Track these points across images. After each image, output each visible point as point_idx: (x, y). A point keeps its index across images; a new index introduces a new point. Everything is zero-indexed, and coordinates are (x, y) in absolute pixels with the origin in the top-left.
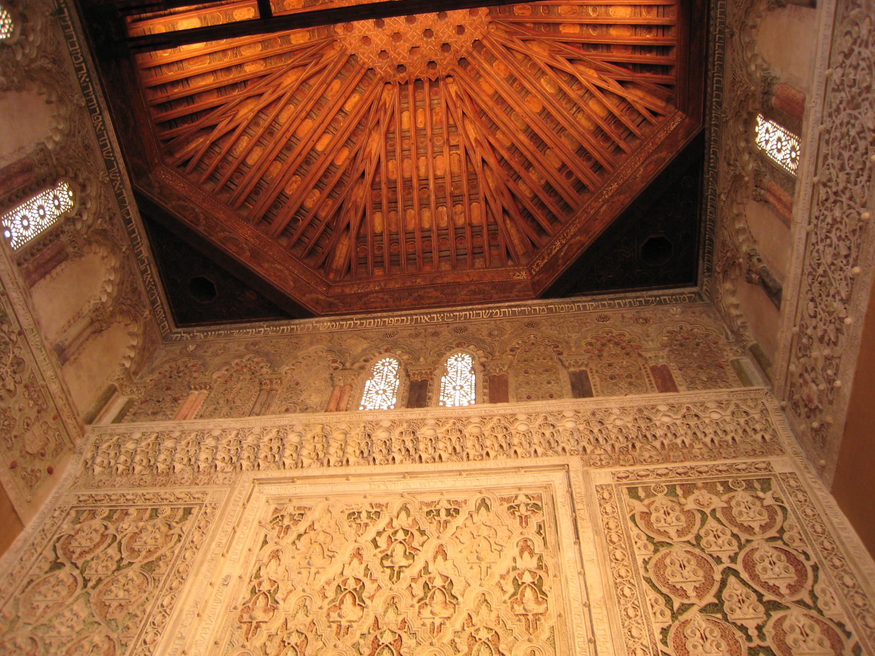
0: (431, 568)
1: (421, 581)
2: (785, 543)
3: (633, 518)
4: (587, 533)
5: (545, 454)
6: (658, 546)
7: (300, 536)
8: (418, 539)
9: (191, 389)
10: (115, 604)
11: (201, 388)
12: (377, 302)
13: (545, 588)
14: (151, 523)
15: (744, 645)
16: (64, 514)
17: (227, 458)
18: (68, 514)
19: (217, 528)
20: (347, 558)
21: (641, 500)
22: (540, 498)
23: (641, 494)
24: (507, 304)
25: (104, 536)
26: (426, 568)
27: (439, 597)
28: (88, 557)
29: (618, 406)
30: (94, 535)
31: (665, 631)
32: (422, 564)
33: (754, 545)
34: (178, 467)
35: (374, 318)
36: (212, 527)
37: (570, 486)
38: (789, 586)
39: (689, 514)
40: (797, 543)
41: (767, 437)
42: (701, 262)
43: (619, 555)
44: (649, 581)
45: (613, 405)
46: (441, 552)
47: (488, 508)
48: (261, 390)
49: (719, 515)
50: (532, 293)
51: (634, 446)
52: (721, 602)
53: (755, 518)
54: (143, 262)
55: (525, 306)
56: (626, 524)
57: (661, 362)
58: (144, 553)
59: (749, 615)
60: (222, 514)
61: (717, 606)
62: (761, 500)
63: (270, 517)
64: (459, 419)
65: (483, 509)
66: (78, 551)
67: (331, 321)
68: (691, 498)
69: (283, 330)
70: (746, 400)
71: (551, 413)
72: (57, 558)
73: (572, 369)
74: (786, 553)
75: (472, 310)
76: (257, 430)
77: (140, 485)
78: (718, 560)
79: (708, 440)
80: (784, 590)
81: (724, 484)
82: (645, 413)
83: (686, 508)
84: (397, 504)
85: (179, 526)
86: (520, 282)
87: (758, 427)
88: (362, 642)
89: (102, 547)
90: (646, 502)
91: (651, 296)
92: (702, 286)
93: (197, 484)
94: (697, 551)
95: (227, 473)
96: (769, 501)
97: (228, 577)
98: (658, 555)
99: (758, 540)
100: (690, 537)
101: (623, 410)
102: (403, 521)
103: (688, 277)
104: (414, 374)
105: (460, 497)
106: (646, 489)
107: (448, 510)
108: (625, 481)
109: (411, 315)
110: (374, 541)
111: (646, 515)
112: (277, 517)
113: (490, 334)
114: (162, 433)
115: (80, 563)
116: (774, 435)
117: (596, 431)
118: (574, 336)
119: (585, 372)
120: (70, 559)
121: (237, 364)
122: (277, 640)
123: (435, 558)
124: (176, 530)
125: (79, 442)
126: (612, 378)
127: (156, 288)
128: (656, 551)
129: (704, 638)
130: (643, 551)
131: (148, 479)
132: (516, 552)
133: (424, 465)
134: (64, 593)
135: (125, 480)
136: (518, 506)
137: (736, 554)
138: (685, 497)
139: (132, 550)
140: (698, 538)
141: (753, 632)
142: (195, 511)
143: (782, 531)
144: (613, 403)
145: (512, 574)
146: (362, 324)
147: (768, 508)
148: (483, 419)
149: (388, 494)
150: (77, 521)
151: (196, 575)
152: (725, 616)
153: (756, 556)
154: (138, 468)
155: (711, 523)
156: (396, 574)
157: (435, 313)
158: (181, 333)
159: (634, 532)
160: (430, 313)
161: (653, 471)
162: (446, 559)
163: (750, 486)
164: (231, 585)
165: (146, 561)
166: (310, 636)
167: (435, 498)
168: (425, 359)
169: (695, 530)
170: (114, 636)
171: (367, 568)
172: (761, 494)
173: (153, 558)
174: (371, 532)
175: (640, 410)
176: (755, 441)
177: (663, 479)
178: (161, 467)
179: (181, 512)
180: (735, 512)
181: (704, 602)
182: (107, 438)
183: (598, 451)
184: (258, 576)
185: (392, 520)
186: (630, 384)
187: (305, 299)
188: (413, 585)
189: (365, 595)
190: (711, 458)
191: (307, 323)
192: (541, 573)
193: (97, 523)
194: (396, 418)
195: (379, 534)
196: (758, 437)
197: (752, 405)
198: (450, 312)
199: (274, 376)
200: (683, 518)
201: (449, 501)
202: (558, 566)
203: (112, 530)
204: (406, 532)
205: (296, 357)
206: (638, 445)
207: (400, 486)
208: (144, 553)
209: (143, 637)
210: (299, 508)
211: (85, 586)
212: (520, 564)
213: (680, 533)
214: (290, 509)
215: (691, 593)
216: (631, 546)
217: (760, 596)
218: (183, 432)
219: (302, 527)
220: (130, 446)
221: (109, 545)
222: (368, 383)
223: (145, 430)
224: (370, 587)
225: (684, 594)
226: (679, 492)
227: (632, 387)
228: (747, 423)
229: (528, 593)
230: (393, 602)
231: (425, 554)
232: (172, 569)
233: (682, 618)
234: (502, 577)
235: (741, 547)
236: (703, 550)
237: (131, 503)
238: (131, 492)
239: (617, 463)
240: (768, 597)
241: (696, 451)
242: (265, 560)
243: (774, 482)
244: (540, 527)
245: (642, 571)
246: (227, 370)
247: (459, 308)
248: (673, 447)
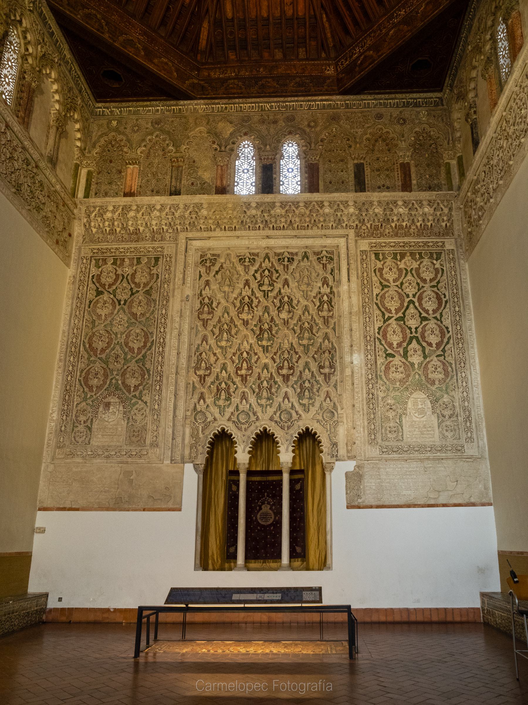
0: (282, 291)
1: (279, 298)
2: (438, 289)
3: (375, 271)
4: (354, 278)
5: (336, 228)
6: (384, 287)
7: (217, 272)
8: (275, 275)
9: (127, 164)
10: (139, 314)
11: (134, 164)
12: (234, 88)
13: (333, 304)
14: (139, 266)
15: (409, 335)
16: (89, 261)
17: (168, 224)
18: (91, 261)
19: (175, 271)
20: (241, 286)
21: (380, 261)
22: (333, 253)
23: (381, 257)
24: (320, 98)
25: (117, 276)
26: (280, 291)
27: (286, 307)
28: (114, 287)
29: (377, 199)
30: (111, 274)
31: (379, 328)
32: (278, 290)
33: (425, 289)
34: (141, 229)
35: (234, 104)
36: (172, 269)
37: (347, 247)
38: (433, 310)
39: (400, 270)
40: (443, 289)
41: (448, 225)
42: (447, 79)
43: (366, 291)
44: (377, 304)
45: (375, 199)
46: (286, 283)
47: (308, 259)
48: (172, 166)
49: (414, 272)
50: (335, 88)
51: (382, 225)
52: (405, 316)
53: (428, 276)
54: (67, 62)
55: (331, 100)
56: (371, 274)
57: (407, 160)
58: (142, 285)
59: (413, 323)
60: (176, 261)
61: (402, 319)
62: (434, 264)
63: (199, 261)
64: (293, 203)
65: (305, 259)
66: (107, 284)
67: (205, 104)
68: (403, 261)
69: (174, 109)
70: (444, 201)
71: (341, 202)
72: (98, 288)
73: (356, 162)
74: (437, 294)
75: (297, 101)
76: (181, 206)
77: (123, 241)
78: (408, 296)
79: (418, 224)
80: (431, 312)
81: (420, 254)
82: (391, 205)
83: (400, 267)
84: (263, 255)
85: (155, 268)
86: (329, 77)
87: (445, 218)
88: (255, 328)
89: (119, 282)
90: (382, 263)
91: (411, 99)
92: (444, 94)
93: (156, 241)
94: (400, 290)
95: (170, 233)
96: (438, 266)
97: (188, 296)
98: (383, 292)
99: (427, 286)
100: (398, 283)
101: (379, 202)
102: (266, 264)
103: (436, 85)
104: (264, 159)
105: (294, 251)
106: (383, 254)
107: (288, 258)
108: (374, 249)
109: (258, 103)
110: (254, 275)
111: (381, 270)
112: (203, 262)
113: (309, 126)
114: (125, 206)
115: (111, 290)
116: (452, 223)
117: (364, 214)
118: (360, 131)
119: (363, 164)
120: (105, 288)
121: (150, 139)
122: (218, 327)
123: (284, 286)
124: (154, 271)
125: (75, 211)
126: (378, 170)
127: (80, 79)
128: (382, 289)
129: (394, 332)
130: (377, 290)
131: (126, 236)
132: (320, 284)
133: (275, 231)
134: (111, 307)
135: (113, 237)
136: (322, 257)
137: (416, 293)
138: (400, 261)
139: (135, 283)
140: (402, 284)
141: (413, 330)
142: (161, 260)
143: (438, 282)
144: (375, 196)
145: (319, 296)
146: (226, 108)
147: (437, 270)
148: (307, 204)
149: (258, 248)
150: (98, 266)
151: (173, 296)
152: (404, 323)
153: (425, 294)
154: (118, 230)
155: (409, 277)
156: (266, 295)
157: (274, 102)
158: (100, 107)
159: (375, 279)
160: (271, 102)
161: (389, 242)
162: (288, 287)
163: (431, 257)
164: (190, 300)
165: (145, 290)
166: (233, 326)
167: (282, 251)
168: (270, 145)
169: (401, 280)
170: (145, 329)
171: (252, 291)
172: (435, 262)
173: (148, 288)
174: (252, 272)
175: (388, 204)
176: (441, 226)
177: (392, 249)
178: (132, 229)
179: (153, 261)
180: (421, 271)
181: (398, 316)
182: (92, 209)
183: (364, 227)
184: (201, 294)
185: (261, 264)
186: (387, 176)
187: (184, 86)
188: (275, 300)
189: (253, 305)
190: (419, 236)
191: (189, 104)
192: (332, 296)
193: (109, 266)
194: (259, 201)
195: (256, 271)
196: (444, 224)
197: (446, 204)
198: (283, 102)
199: (178, 155)
200: (397, 273)
201: (288, 253)
202: (338, 292)
203: (119, 272)
204: (269, 271)
205: (188, 138)
206: (384, 224)
207: (264, 243)
208: (142, 285)
209: (158, 329)
210: (213, 255)
211: (120, 304)
212: (322, 291)
213: (394, 281)
214: (209, 256)
215: (393, 311)
216: (372, 286)
217: (421, 314)
218: (138, 206)
219: (216, 268)
220: (109, 215)
221: (122, 280)
222: (237, 163)
223: (114, 204)
224: (255, 302)
225: (390, 311)
226: (399, 257)
227: (387, 178)
228: (440, 215)
229: (326, 306)
230: (266, 309)
231: (278, 285)
232: (160, 295)
233: (387, 323)
234: (314, 297)
235: (419, 290)
236: (402, 290)
237: (123, 254)
238: (121, 246)
239: (371, 235)
240: (424, 314)
241: (412, 231)
242: (203, 286)
243: (443, 255)
244: (332, 270)
245: (375, 300)
246: (145, 146)
247: (289, 99)
248: (401, 227)
